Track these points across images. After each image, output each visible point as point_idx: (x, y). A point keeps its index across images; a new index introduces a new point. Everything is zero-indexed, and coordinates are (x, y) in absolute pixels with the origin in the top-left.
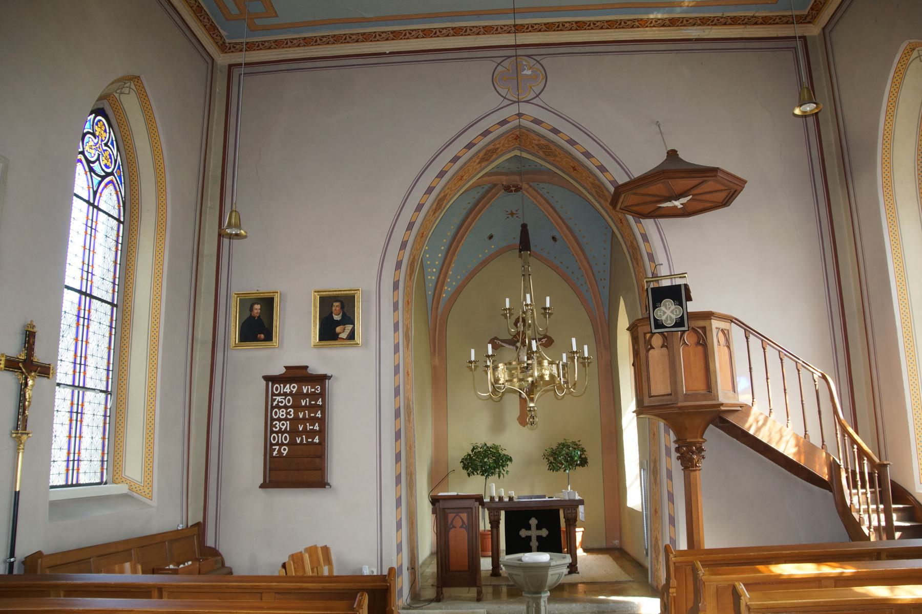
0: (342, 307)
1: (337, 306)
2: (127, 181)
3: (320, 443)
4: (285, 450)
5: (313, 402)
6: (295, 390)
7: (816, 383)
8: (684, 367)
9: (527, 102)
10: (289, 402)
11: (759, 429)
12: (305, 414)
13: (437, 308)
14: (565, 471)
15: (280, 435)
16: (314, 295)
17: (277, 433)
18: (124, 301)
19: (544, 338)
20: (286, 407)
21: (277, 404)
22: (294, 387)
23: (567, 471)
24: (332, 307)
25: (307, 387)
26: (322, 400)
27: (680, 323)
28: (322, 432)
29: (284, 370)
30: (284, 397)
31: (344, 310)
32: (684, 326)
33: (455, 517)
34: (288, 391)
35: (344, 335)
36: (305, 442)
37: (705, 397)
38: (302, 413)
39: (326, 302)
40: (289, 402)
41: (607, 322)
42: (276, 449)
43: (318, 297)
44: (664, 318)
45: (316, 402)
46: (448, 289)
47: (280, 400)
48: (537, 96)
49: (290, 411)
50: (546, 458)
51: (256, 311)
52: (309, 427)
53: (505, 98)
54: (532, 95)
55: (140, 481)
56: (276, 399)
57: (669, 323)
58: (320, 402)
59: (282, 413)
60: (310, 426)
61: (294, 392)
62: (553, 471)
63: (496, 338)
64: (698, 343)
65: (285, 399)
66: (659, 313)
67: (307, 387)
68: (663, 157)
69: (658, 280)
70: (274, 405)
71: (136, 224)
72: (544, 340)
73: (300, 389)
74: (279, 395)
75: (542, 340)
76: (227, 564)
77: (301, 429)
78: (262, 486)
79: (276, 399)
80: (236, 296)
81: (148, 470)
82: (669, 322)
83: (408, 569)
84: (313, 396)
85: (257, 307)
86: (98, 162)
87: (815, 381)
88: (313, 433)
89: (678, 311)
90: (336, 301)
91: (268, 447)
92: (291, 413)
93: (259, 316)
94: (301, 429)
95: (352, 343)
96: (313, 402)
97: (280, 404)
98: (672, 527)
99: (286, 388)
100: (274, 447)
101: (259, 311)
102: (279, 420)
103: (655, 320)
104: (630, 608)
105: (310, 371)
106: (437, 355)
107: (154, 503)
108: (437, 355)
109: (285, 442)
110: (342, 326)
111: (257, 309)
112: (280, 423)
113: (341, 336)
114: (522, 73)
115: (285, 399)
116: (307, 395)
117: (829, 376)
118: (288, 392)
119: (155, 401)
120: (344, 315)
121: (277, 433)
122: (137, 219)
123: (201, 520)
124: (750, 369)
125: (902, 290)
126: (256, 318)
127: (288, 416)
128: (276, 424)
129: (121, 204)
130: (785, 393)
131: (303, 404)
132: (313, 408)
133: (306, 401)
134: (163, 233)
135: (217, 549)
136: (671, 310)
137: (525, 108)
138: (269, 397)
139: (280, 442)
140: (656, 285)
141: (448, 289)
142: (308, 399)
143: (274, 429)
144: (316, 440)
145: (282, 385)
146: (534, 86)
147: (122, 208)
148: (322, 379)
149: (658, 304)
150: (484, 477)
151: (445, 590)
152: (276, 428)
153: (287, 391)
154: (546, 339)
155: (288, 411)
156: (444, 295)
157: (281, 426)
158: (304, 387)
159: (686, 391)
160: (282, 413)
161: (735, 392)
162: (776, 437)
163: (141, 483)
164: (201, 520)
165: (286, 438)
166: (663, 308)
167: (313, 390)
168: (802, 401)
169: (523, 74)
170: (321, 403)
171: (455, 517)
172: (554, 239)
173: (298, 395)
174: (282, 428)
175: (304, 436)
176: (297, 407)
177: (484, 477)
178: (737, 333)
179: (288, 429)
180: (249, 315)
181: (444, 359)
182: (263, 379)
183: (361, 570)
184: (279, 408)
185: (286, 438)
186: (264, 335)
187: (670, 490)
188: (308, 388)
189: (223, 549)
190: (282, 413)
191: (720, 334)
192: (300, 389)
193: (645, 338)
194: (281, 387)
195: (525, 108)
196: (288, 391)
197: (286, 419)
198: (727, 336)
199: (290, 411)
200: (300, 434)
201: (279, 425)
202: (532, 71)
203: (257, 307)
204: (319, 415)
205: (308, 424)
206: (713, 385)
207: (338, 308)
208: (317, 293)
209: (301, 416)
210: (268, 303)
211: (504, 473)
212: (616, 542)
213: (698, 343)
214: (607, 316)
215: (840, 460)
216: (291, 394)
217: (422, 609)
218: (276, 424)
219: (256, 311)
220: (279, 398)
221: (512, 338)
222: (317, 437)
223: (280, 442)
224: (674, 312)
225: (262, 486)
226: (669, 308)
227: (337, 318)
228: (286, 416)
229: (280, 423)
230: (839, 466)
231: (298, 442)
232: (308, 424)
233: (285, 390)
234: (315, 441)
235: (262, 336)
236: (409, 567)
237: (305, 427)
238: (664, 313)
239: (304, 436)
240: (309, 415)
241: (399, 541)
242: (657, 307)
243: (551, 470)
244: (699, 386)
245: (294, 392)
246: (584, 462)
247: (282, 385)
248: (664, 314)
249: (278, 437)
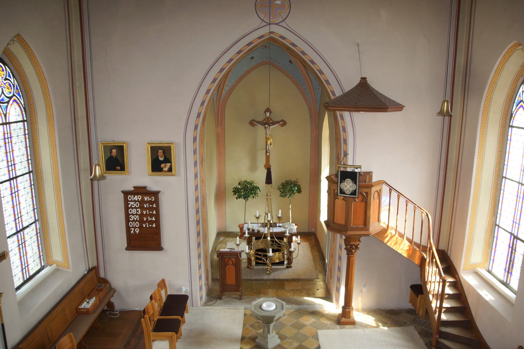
0: (164, 153)
1: (161, 152)
2: (24, 95)
3: (156, 227)
4: (137, 230)
5: (151, 206)
6: (140, 199)
7: (423, 217)
8: (353, 213)
9: (277, 24)
10: (137, 205)
11: (388, 241)
12: (146, 212)
13: (220, 101)
14: (289, 197)
15: (134, 222)
16: (147, 146)
17: (132, 221)
18: (36, 167)
19: (281, 121)
20: (136, 208)
21: (131, 206)
22: (139, 197)
23: (290, 198)
24: (158, 153)
25: (147, 197)
26: (155, 224)
27: (354, 193)
28: (158, 221)
29: (133, 189)
30: (134, 203)
31: (165, 155)
32: (356, 195)
33: (229, 260)
34: (136, 199)
35: (166, 169)
36: (148, 226)
37: (362, 229)
38: (145, 211)
39: (154, 150)
40: (137, 205)
41: (318, 112)
42: (132, 230)
43: (150, 146)
44: (345, 189)
45: (153, 205)
46: (226, 88)
47: (132, 204)
48: (284, 20)
49: (139, 210)
50: (279, 189)
51: (114, 153)
52: (149, 219)
53: (263, 20)
54: (281, 19)
55: (62, 261)
56: (130, 204)
57: (348, 192)
58: (154, 206)
59: (134, 211)
60: (150, 218)
61: (139, 200)
62: (282, 197)
63: (253, 120)
64: (362, 201)
65: (135, 203)
66: (343, 186)
67: (147, 197)
68: (356, 81)
69: (346, 167)
70: (129, 207)
71: (35, 118)
72: (281, 123)
73: (143, 200)
74: (132, 201)
75: (280, 123)
76: (113, 286)
77: (145, 220)
78: (127, 249)
79: (130, 204)
80: (101, 144)
81: (65, 255)
82: (348, 191)
83: (205, 285)
84: (150, 202)
85: (114, 151)
86: (6, 104)
87: (422, 216)
88: (151, 222)
89: (354, 187)
90: (161, 149)
91: (128, 229)
92: (139, 211)
93: (116, 156)
94: (145, 220)
95: (170, 174)
96: (151, 206)
97: (132, 206)
98: (339, 272)
99: (135, 198)
100: (131, 229)
101: (116, 153)
102: (133, 215)
103: (341, 189)
104: (314, 308)
105: (148, 189)
106: (219, 127)
107: (71, 270)
108: (219, 127)
109: (138, 226)
110: (164, 164)
111: (114, 152)
112: (132, 213)
113: (164, 169)
114: (275, 2)
115: (135, 203)
116: (147, 202)
117: (430, 214)
118: (136, 200)
119: (63, 219)
120: (165, 157)
121: (132, 221)
122: (34, 116)
123: (96, 265)
124: (389, 209)
125: (478, 174)
126: (114, 157)
127: (138, 213)
128: (131, 217)
129: (23, 110)
130: (406, 221)
131: (145, 207)
132: (151, 209)
133: (147, 205)
134: (52, 121)
135: (106, 278)
136: (350, 185)
137: (274, 28)
138: (126, 202)
139: (134, 226)
140: (345, 170)
141: (226, 88)
142: (148, 204)
143: (130, 219)
144: (154, 226)
145: (133, 196)
146: (282, 13)
147: (24, 112)
148: (156, 194)
149: (343, 181)
150: (245, 200)
151: (224, 293)
152: (132, 219)
153: (135, 199)
154: (282, 122)
155: (137, 210)
156: (224, 92)
157: (134, 218)
158: (145, 197)
159: (353, 225)
160: (134, 211)
161: (379, 221)
162: (396, 244)
163: (62, 262)
164: (96, 265)
165: (137, 224)
166: (345, 183)
167: (150, 199)
168: (413, 227)
169: (275, 4)
170: (155, 206)
171: (229, 260)
172: (290, 61)
173: (142, 202)
174: (135, 219)
175: (147, 224)
176: (142, 208)
177: (245, 200)
178: (385, 189)
179: (138, 220)
180: (110, 156)
181: (223, 130)
182: (121, 193)
183: (181, 289)
184: (133, 208)
185: (137, 224)
186: (120, 167)
187: (340, 255)
188: (147, 198)
189: (110, 278)
190: (134, 211)
191: (376, 193)
192: (143, 200)
193: (334, 192)
194: (132, 197)
195: (274, 28)
196: (136, 199)
197: (137, 214)
198: (379, 193)
199: (139, 210)
200: (145, 222)
201: (133, 217)
202: (281, 2)
203: (114, 151)
204: (154, 212)
205: (149, 217)
206: (367, 223)
207: (162, 154)
208: (149, 145)
209: (145, 213)
210: (120, 149)
211: (256, 197)
212: (313, 230)
213: (362, 201)
214: (318, 109)
215: (427, 256)
216: (138, 201)
217: (212, 306)
218: (131, 217)
219: (114, 153)
220: (132, 203)
221: (263, 121)
222: (154, 224)
223: (134, 226)
224: (352, 187)
225: (127, 249)
226: (349, 184)
227: (161, 159)
228: (137, 213)
229: (132, 213)
230: (425, 260)
231: (144, 226)
232: (149, 217)
233: (135, 199)
234: (153, 226)
235: (119, 168)
236: (206, 283)
237: (147, 219)
238: (346, 186)
239: (147, 224)
240: (149, 212)
241: (201, 281)
242: (342, 182)
243: (281, 197)
244: (360, 223)
245: (139, 200)
246: (299, 191)
247: (133, 196)
248: (346, 187)
249: (133, 223)
